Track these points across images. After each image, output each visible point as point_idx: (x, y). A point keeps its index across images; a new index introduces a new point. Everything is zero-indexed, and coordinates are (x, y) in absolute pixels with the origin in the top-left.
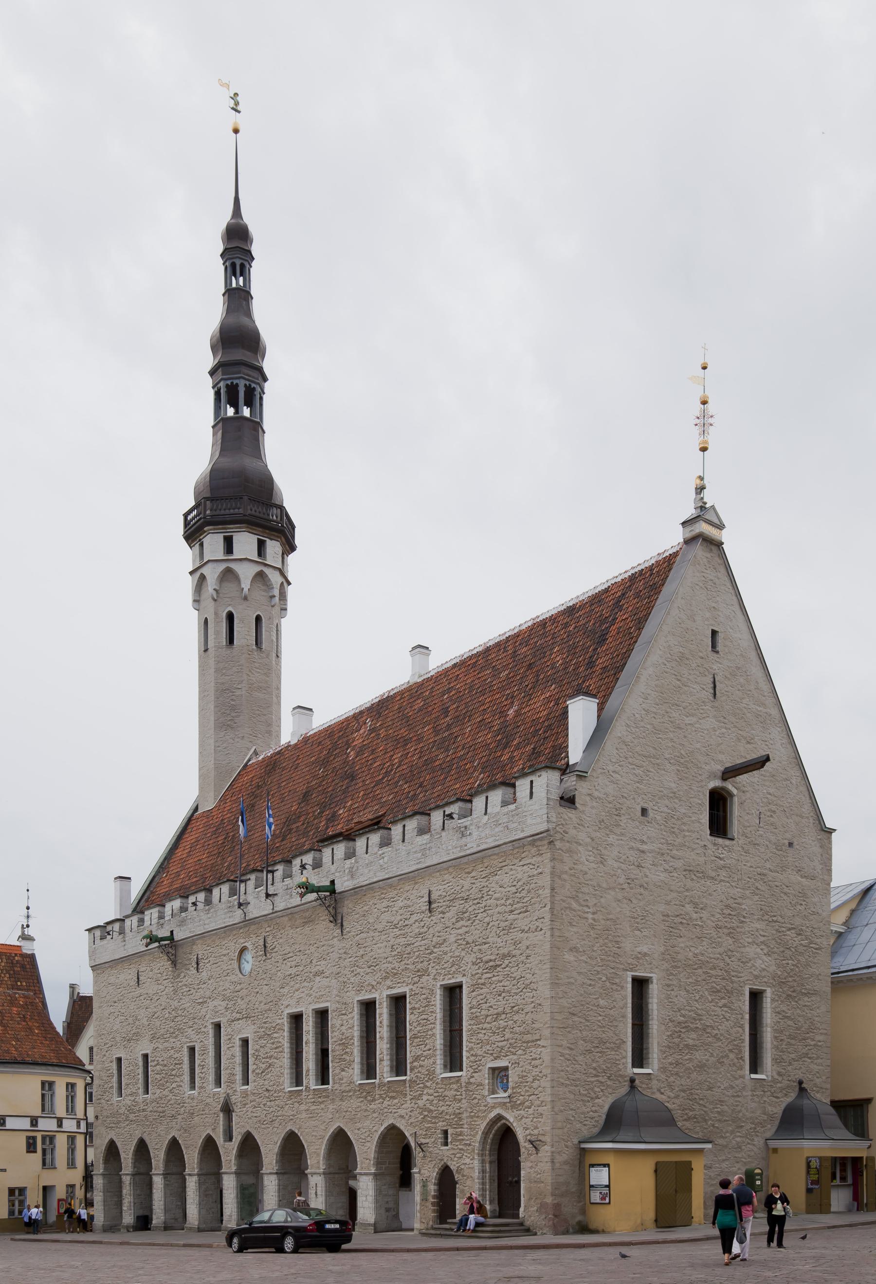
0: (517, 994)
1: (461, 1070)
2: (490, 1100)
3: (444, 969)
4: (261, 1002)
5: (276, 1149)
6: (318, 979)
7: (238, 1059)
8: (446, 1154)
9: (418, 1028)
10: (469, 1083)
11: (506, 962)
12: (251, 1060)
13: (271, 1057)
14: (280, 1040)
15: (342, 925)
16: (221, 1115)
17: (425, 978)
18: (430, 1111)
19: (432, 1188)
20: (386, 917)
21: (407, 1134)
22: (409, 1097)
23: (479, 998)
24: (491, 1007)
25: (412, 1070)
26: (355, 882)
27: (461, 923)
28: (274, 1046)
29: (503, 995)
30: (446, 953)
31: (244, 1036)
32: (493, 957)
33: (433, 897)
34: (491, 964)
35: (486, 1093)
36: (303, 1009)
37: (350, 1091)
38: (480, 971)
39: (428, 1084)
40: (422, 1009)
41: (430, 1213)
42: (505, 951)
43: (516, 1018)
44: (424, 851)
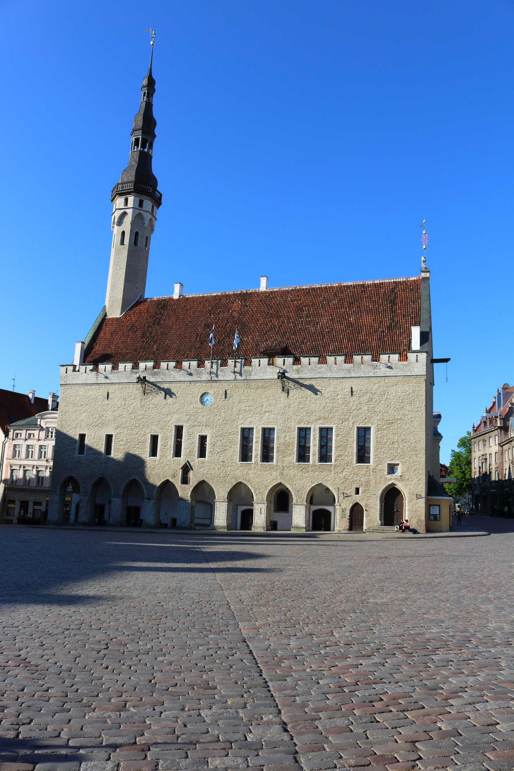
1: (369, 463)
2: (389, 476)
4: (219, 420)
5: (228, 490)
6: (267, 414)
8: (357, 499)
9: (341, 443)
10: (375, 469)
11: (399, 422)
15: (288, 393)
16: (181, 470)
17: (346, 423)
19: (348, 513)
21: (331, 489)
22: (333, 472)
25: (335, 461)
26: (300, 375)
27: (371, 403)
31: (203, 434)
33: (353, 390)
35: (386, 473)
38: (383, 423)
39: (348, 467)
41: (346, 523)
42: (399, 417)
43: (404, 444)
44: (349, 371)
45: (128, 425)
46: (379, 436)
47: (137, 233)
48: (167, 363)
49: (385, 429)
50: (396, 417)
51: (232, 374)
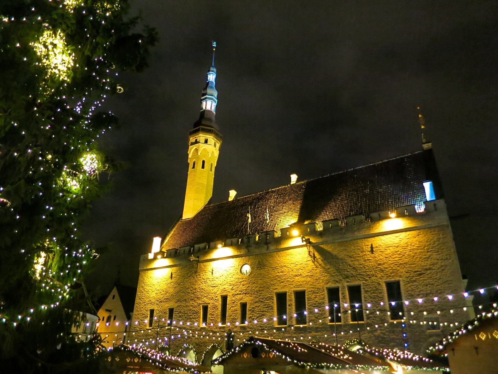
0: (438, 285)
3: (387, 274)
6: (297, 278)
7: (239, 312)
12: (248, 313)
13: (263, 312)
14: (270, 304)
18: (383, 338)
20: (345, 253)
23: (412, 287)
24: (422, 291)
28: (266, 306)
29: (429, 286)
30: (386, 268)
32: (418, 270)
34: (418, 273)
36: (287, 291)
37: (322, 328)
40: (372, 291)
45: (185, 298)
46: (410, 289)
47: (204, 162)
48: (215, 243)
49: (415, 281)
50: (425, 268)
51: (266, 246)
